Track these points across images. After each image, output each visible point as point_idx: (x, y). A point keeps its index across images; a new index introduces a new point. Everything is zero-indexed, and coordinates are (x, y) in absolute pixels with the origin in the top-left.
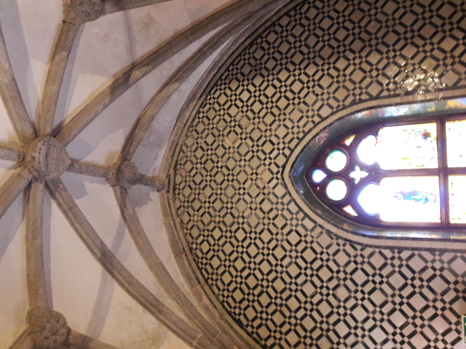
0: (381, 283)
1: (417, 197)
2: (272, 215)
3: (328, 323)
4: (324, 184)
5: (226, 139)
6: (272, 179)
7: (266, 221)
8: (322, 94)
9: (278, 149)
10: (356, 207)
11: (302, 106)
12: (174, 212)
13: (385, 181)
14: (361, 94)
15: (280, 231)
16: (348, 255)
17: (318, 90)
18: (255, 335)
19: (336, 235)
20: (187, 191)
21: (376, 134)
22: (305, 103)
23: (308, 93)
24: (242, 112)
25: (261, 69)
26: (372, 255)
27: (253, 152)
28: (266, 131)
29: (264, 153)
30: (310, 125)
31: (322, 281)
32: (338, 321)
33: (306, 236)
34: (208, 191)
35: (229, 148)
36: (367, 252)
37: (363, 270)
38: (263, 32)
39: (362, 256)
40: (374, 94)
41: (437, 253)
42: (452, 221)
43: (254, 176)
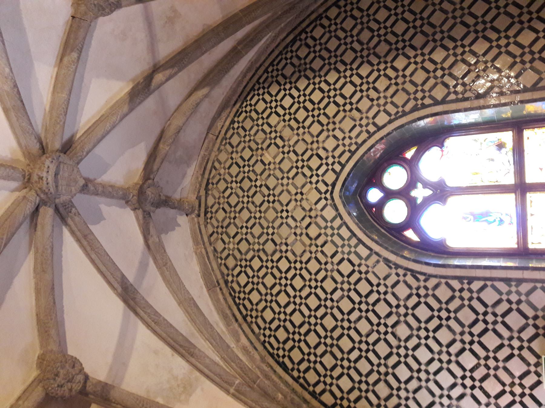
0: (448, 319)
1: (490, 219)
2: (320, 242)
3: (386, 366)
5: (266, 154)
6: (320, 199)
8: (378, 99)
9: (327, 164)
10: (418, 231)
11: (355, 113)
12: (206, 239)
13: (452, 200)
14: (423, 98)
15: (329, 260)
16: (410, 287)
17: (373, 94)
18: (301, 381)
19: (395, 264)
20: (221, 215)
21: (441, 146)
22: (358, 109)
23: (362, 97)
24: (284, 121)
25: (305, 70)
26: (436, 286)
27: (297, 168)
28: (312, 143)
29: (310, 169)
30: (364, 135)
31: (379, 317)
32: (398, 363)
33: (359, 265)
34: (245, 215)
35: (270, 164)
37: (426, 304)
38: (308, 26)
39: (426, 288)
40: (439, 97)
41: (513, 283)
42: (531, 246)
43: (299, 197)
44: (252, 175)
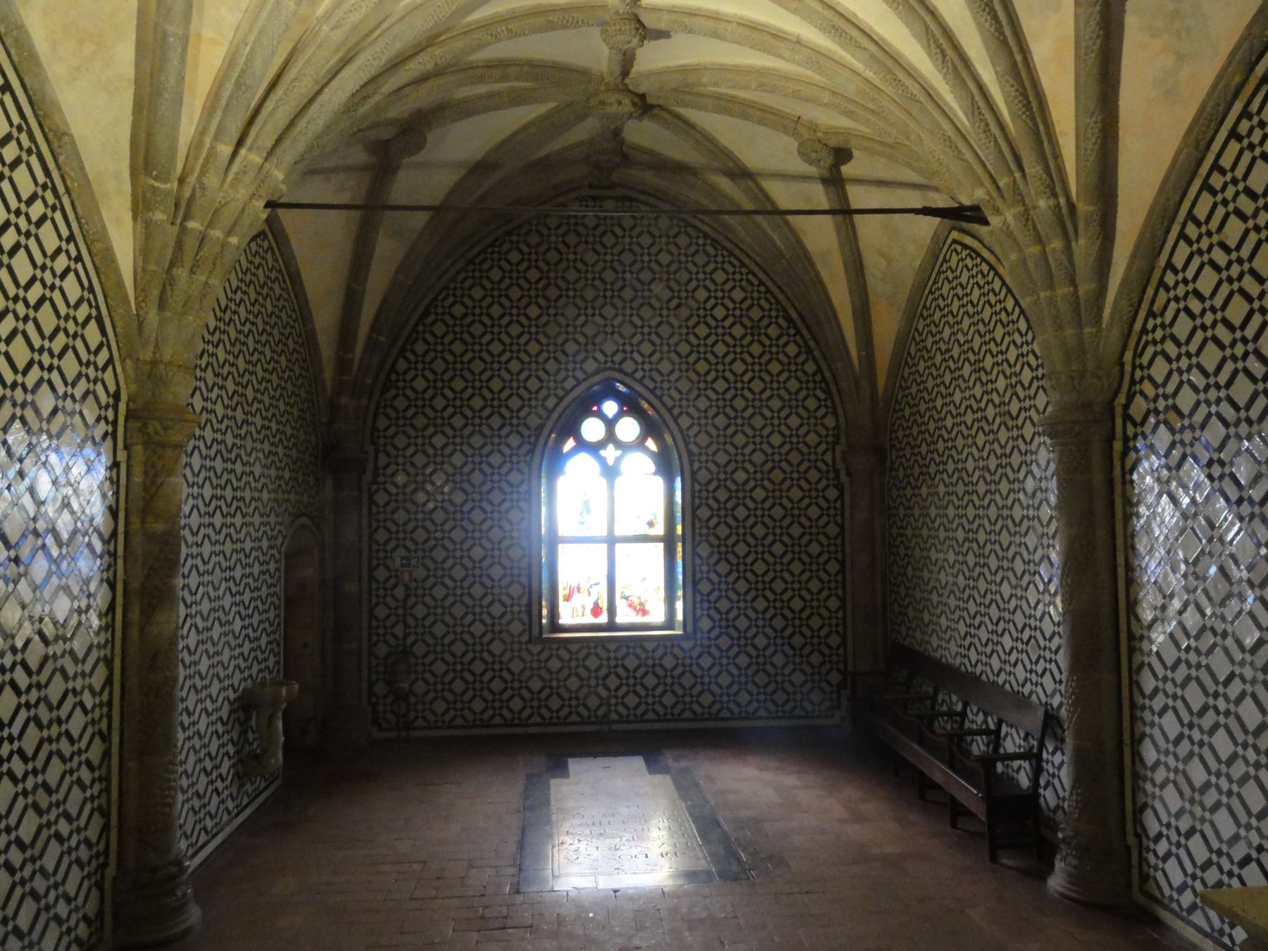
4: (600, 415)
7: (552, 348)
10: (574, 451)
11: (696, 393)
13: (603, 481)
42: (560, 546)
43: (609, 330)
44: (637, 266)
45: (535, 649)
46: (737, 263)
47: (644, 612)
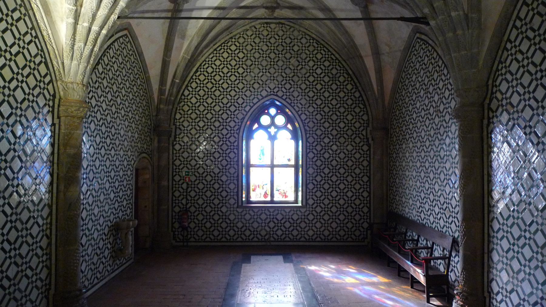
1: (261, 155)
2: (251, 89)
4: (268, 114)
5: (295, 60)
8: (313, 115)
9: (286, 92)
10: (257, 129)
13: (269, 142)
16: (234, 127)
17: (315, 113)
18: (192, 80)
20: (265, 33)
24: (310, 70)
25: (333, 81)
28: (297, 85)
35: (289, 62)
36: (235, 135)
38: (354, 82)
39: (234, 133)
42: (251, 168)
43: (272, 78)
45: (240, 210)
46: (327, 51)
47: (286, 197)
